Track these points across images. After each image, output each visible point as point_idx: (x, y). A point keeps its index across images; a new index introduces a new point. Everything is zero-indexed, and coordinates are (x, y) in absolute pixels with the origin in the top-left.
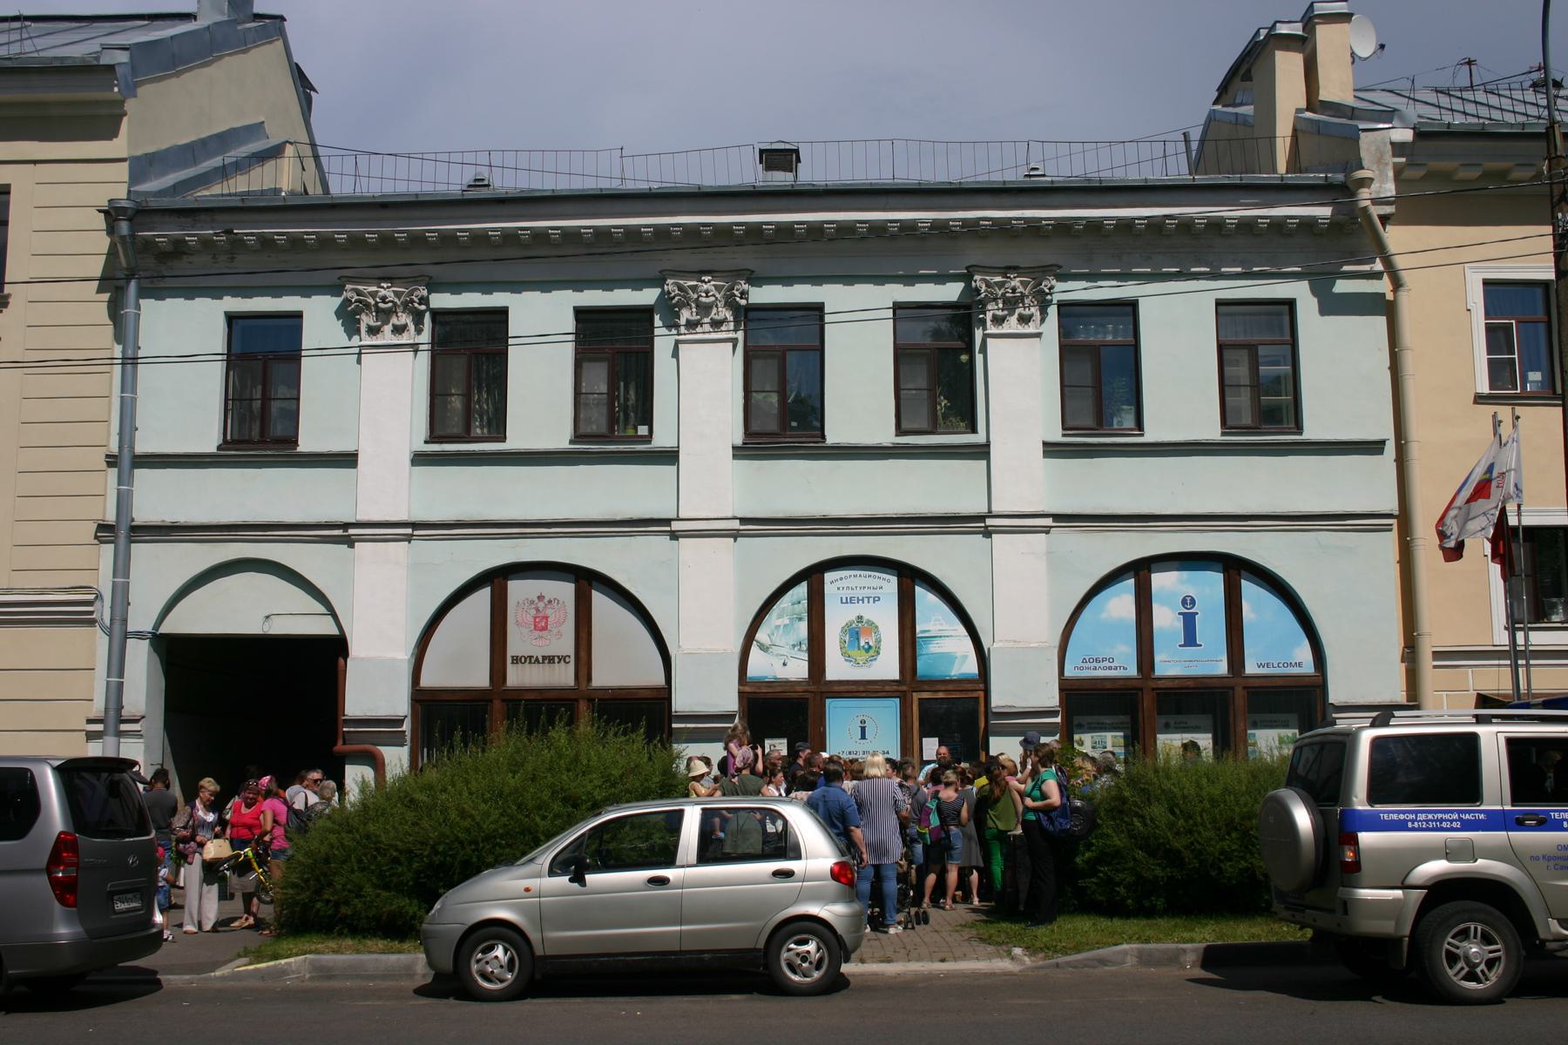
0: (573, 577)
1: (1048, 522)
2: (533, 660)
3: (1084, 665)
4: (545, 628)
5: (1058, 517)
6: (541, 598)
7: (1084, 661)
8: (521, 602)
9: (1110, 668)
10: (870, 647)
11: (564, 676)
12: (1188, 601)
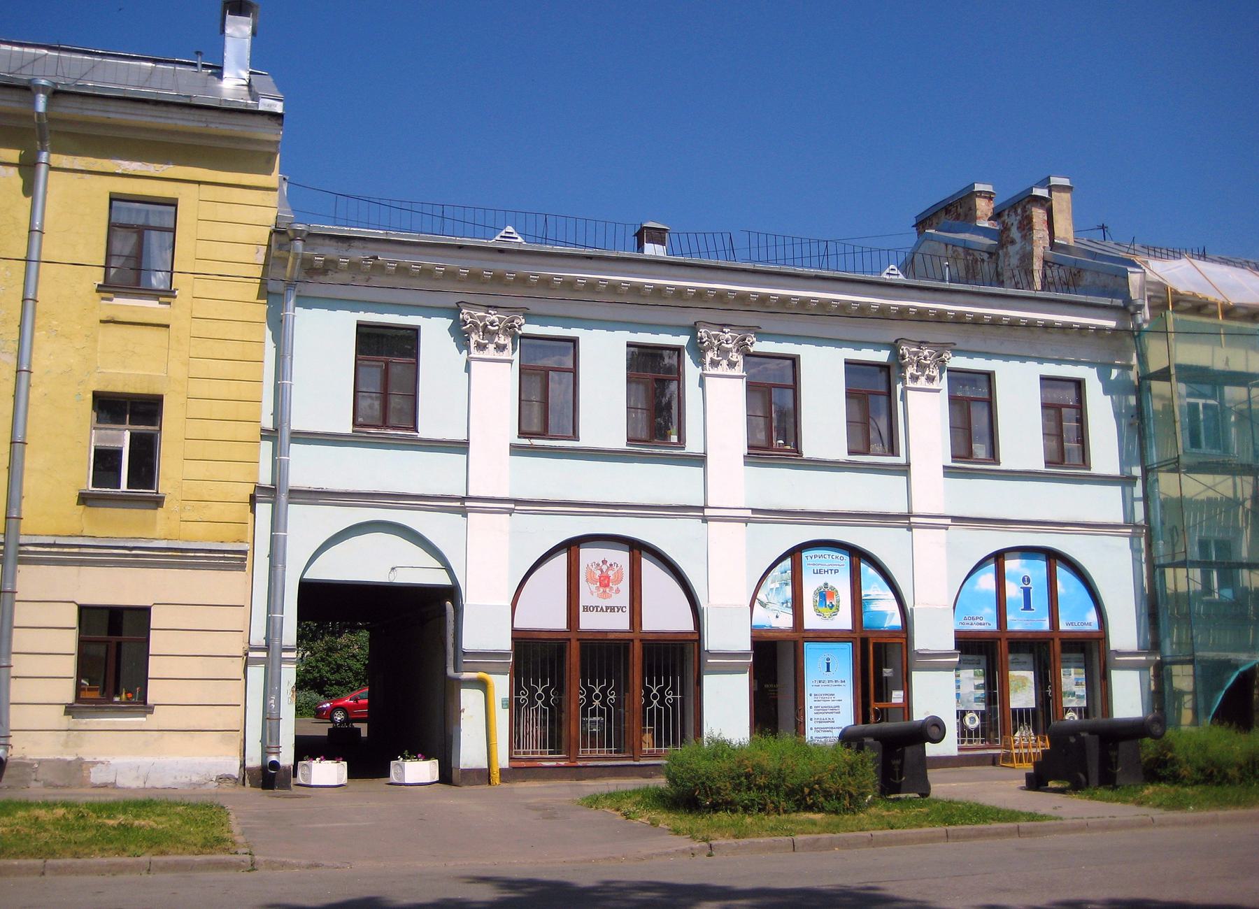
0: (627, 547)
1: (948, 521)
2: (599, 609)
3: (966, 622)
4: (607, 585)
5: (954, 519)
6: (604, 562)
7: (965, 619)
8: (590, 565)
9: (981, 624)
10: (833, 606)
11: (620, 622)
12: (1026, 580)
